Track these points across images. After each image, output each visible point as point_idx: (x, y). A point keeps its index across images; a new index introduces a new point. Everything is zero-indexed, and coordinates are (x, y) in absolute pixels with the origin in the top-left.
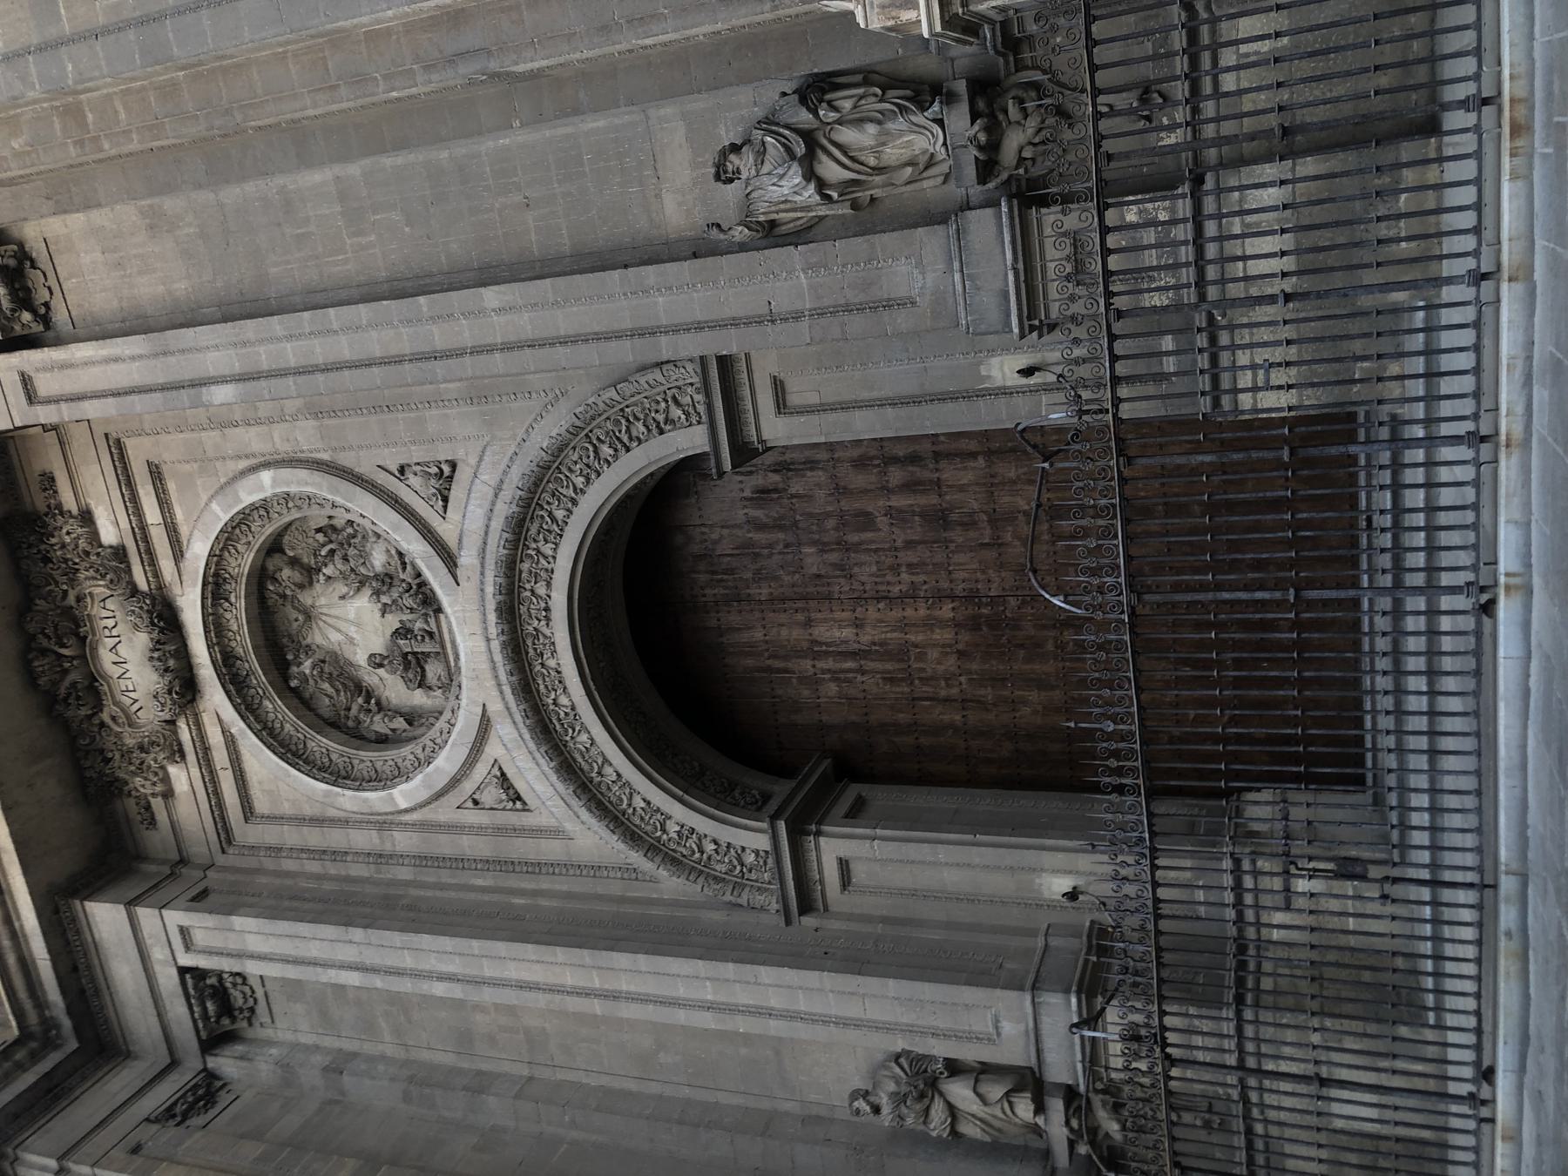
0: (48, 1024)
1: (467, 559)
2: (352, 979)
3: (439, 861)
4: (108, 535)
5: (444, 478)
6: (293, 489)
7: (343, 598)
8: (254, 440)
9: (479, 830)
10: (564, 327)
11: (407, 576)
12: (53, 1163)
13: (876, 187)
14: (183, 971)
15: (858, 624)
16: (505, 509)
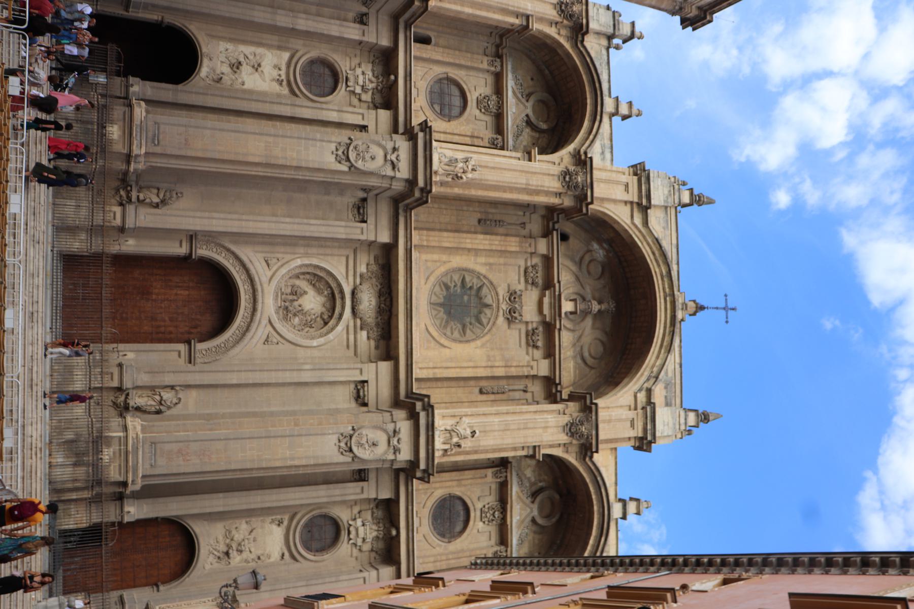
0: (405, 211)
1: (265, 322)
2: (313, 221)
3: (290, 245)
4: (364, 334)
5: (267, 341)
6: (308, 341)
7: (313, 309)
8: (316, 353)
9: (278, 253)
10: (220, 374)
11: (290, 315)
12: (393, 187)
13: (150, 393)
14: (365, 222)
15: (176, 294)
16: (249, 335)
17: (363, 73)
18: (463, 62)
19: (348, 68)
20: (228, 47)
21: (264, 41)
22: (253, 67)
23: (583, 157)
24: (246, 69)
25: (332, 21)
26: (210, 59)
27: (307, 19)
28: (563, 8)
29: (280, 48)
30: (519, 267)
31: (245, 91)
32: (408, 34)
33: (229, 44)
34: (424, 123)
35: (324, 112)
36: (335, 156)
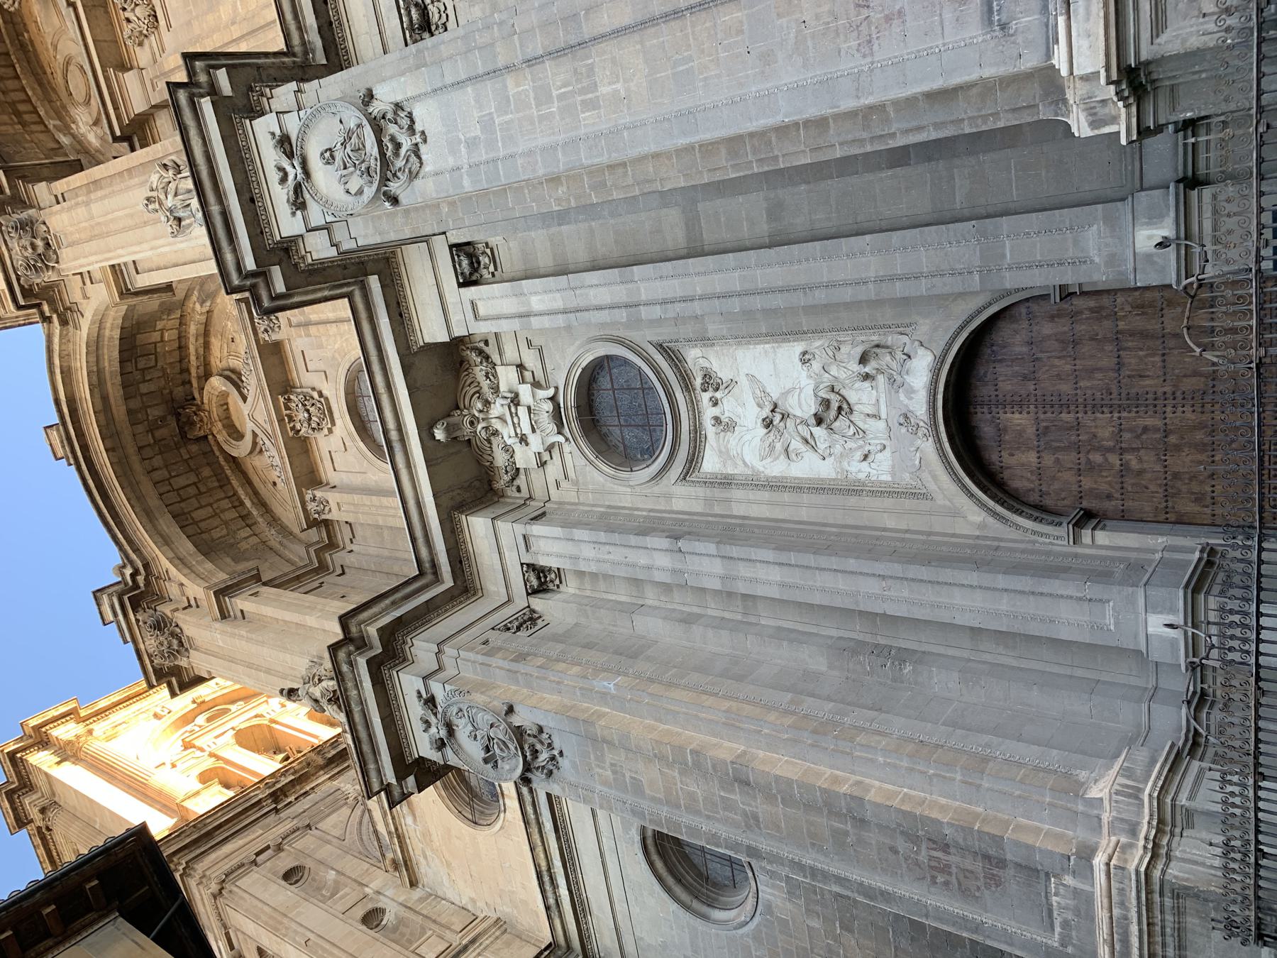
17: (523, 440)
18: (366, 500)
19: (567, 448)
20: (865, 463)
21: (766, 495)
22: (784, 417)
23: (46, 308)
24: (804, 406)
25: (593, 568)
26: (906, 417)
27: (649, 568)
28: (175, 642)
29: (726, 482)
30: (169, 27)
31: (796, 334)
32: (424, 553)
33: (862, 476)
34: (266, 303)
35: (558, 302)
36: (418, 127)
